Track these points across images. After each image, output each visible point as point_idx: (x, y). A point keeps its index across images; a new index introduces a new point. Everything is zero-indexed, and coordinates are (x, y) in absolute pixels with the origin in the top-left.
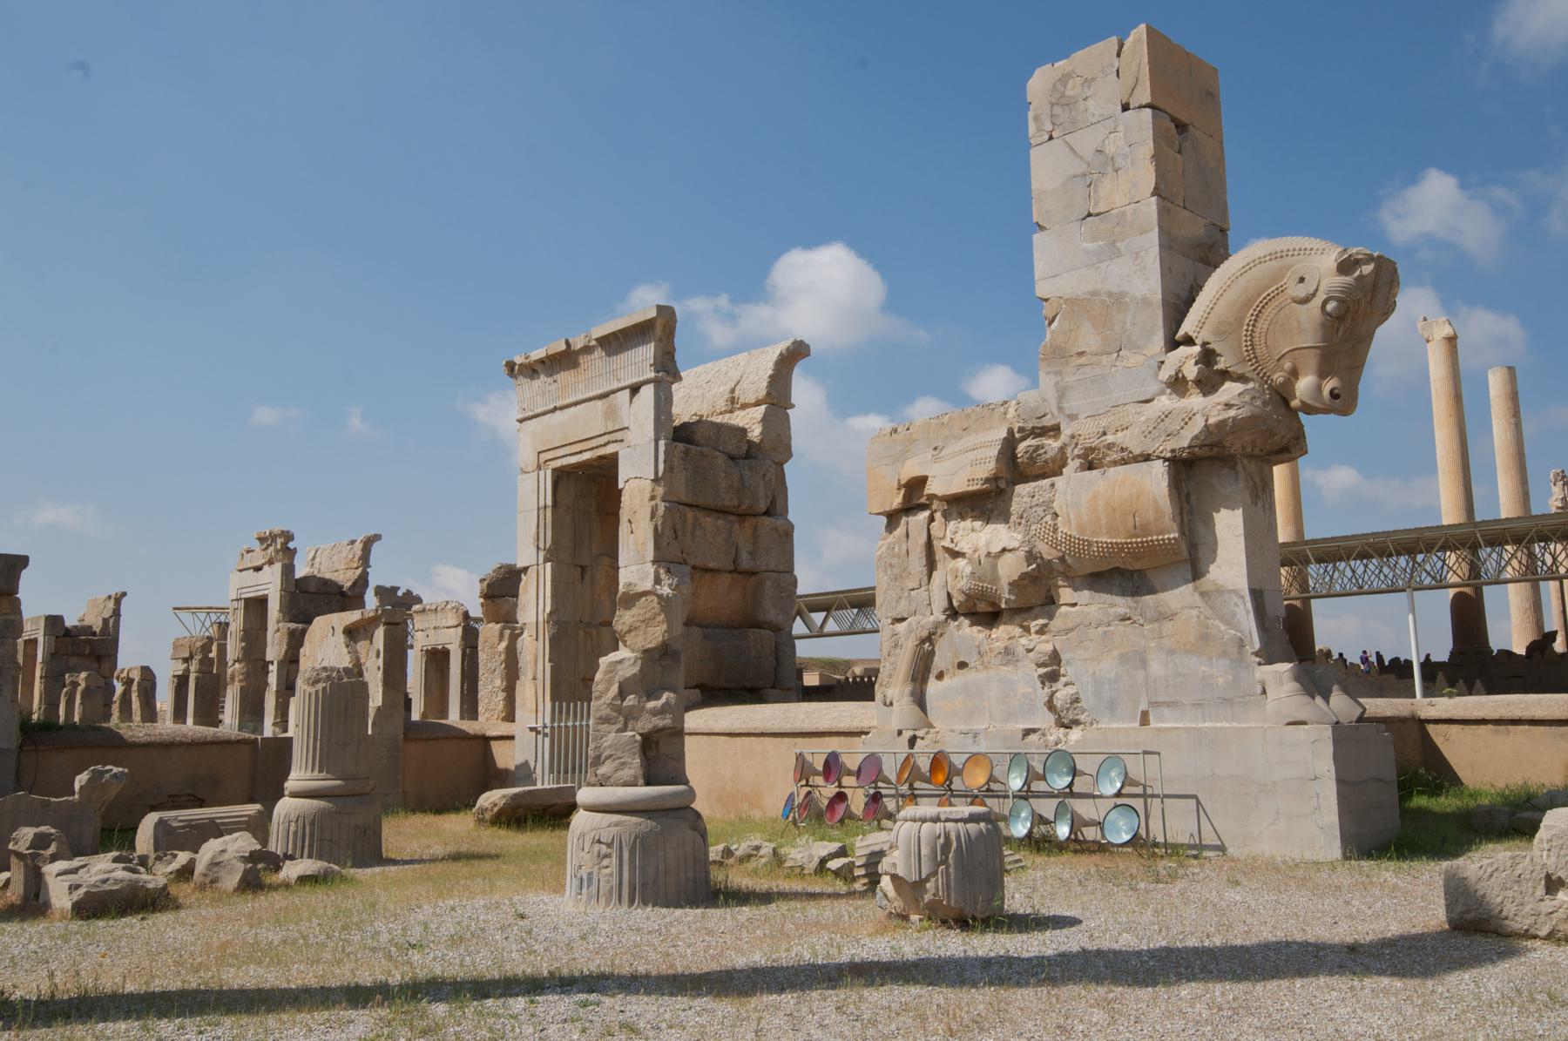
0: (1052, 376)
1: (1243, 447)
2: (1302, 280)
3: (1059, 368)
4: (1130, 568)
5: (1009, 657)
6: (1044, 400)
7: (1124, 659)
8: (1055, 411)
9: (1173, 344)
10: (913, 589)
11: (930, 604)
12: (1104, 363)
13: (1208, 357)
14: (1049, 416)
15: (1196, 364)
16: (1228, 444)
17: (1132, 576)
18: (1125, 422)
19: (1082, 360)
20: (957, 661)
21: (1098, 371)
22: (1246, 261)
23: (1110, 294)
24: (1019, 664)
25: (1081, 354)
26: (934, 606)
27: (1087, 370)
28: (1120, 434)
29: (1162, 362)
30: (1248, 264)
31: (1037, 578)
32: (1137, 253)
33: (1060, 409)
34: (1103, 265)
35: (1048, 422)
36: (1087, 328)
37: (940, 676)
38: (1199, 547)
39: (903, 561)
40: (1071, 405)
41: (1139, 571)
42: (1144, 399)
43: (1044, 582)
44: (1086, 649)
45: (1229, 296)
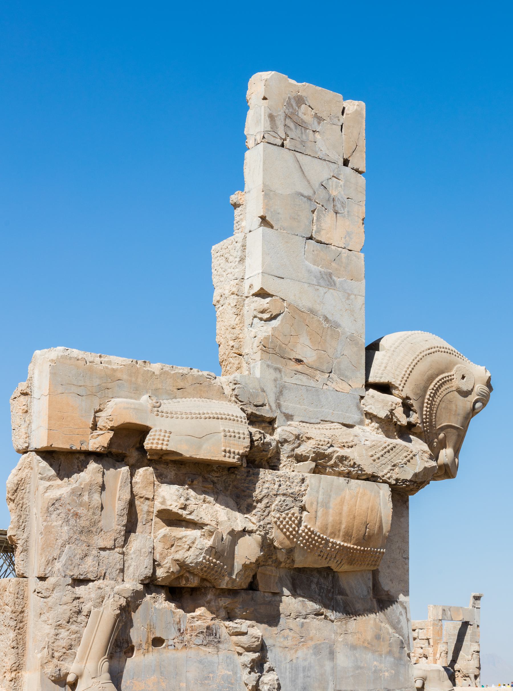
0: (272, 371)
3: (279, 366)
6: (263, 391)
10: (104, 549)
11: (122, 571)
12: (317, 378)
14: (267, 407)
19: (299, 367)
21: (312, 383)
24: (220, 646)
26: (129, 572)
27: (304, 378)
29: (362, 397)
33: (279, 406)
36: (304, 339)
39: (94, 514)
42: (347, 423)
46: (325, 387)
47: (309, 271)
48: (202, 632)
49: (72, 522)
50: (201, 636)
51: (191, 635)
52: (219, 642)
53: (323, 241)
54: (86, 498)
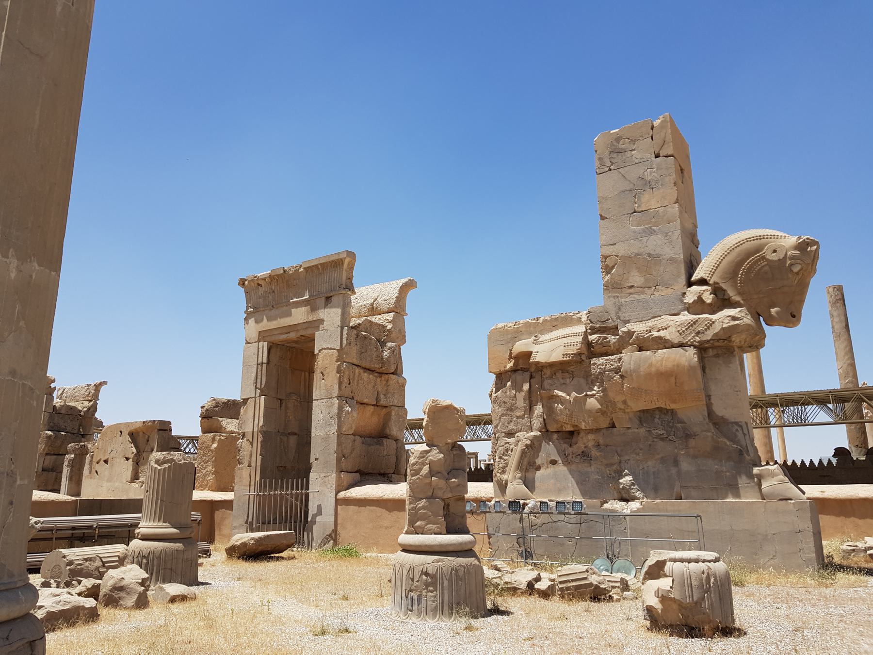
0: (611, 299)
1: (740, 341)
2: (775, 251)
4: (668, 408)
5: (585, 458)
7: (663, 460)
8: (615, 318)
9: (690, 284)
13: (717, 290)
15: (710, 294)
16: (733, 339)
17: (667, 412)
18: (664, 325)
19: (632, 290)
20: (549, 459)
22: (739, 240)
23: (650, 255)
24: (592, 462)
25: (631, 287)
28: (661, 331)
29: (685, 293)
30: (739, 242)
31: (605, 412)
32: (667, 233)
33: (619, 317)
34: (645, 239)
35: (610, 324)
37: (538, 468)
38: (711, 397)
40: (625, 315)
41: (672, 409)
43: (609, 414)
44: (638, 454)
45: (729, 258)
46: (653, 296)
47: (635, 232)
48: (579, 455)
49: (503, 406)
50: (579, 457)
51: (572, 457)
52: (591, 460)
53: (643, 210)
54: (508, 393)
